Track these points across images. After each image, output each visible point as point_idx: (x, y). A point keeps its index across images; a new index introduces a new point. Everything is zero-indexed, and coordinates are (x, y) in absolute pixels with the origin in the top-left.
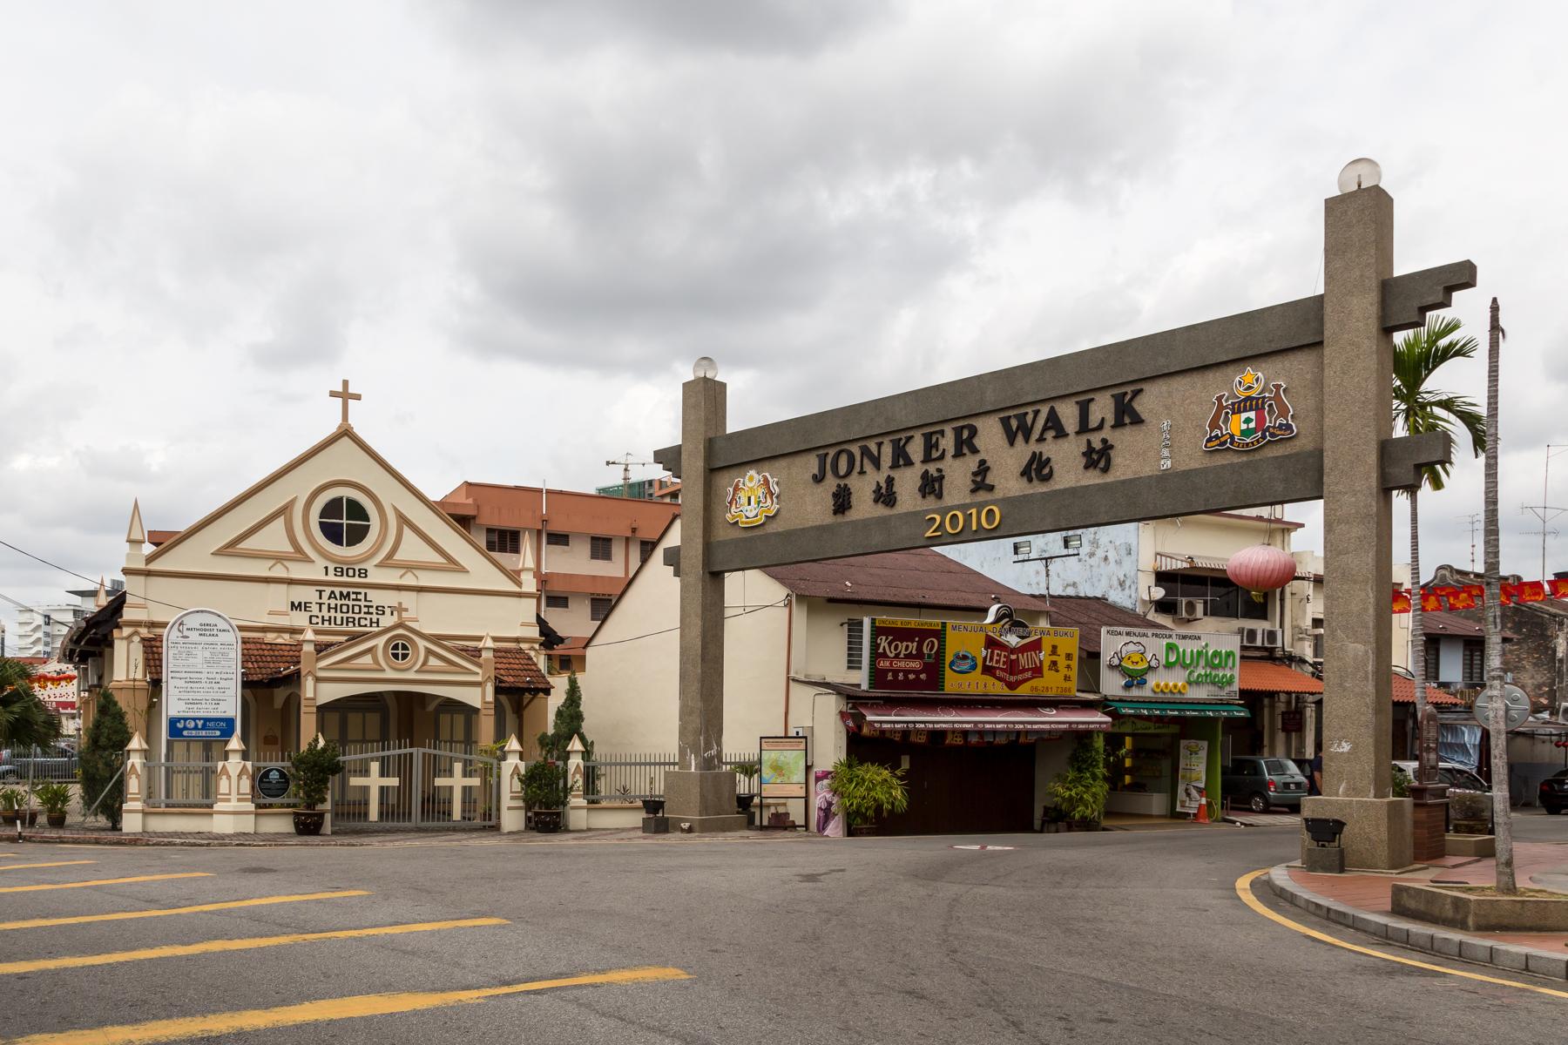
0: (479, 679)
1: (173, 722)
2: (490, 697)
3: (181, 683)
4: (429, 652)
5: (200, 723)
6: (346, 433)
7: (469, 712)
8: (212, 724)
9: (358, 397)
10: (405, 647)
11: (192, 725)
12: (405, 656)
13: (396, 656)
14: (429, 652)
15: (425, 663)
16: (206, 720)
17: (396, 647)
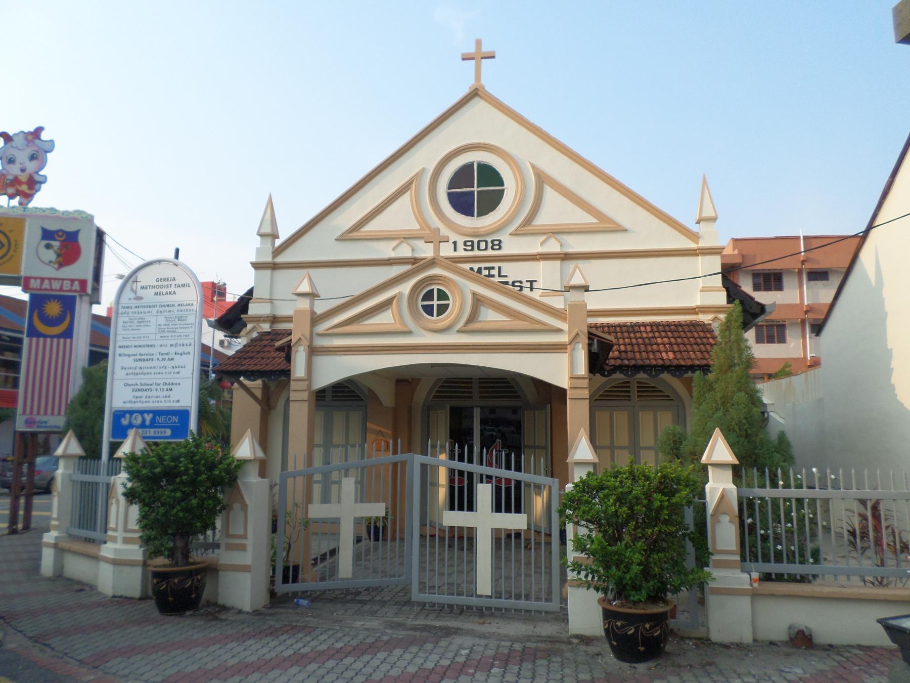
0: (564, 338)
1: (118, 415)
2: (582, 368)
3: (129, 362)
4: (478, 301)
5: (148, 418)
6: (475, 93)
7: (551, 396)
8: (161, 420)
9: (479, 43)
10: (442, 295)
11: (139, 421)
12: (442, 309)
13: (429, 310)
14: (478, 301)
15: (473, 317)
16: (157, 413)
17: (429, 296)
